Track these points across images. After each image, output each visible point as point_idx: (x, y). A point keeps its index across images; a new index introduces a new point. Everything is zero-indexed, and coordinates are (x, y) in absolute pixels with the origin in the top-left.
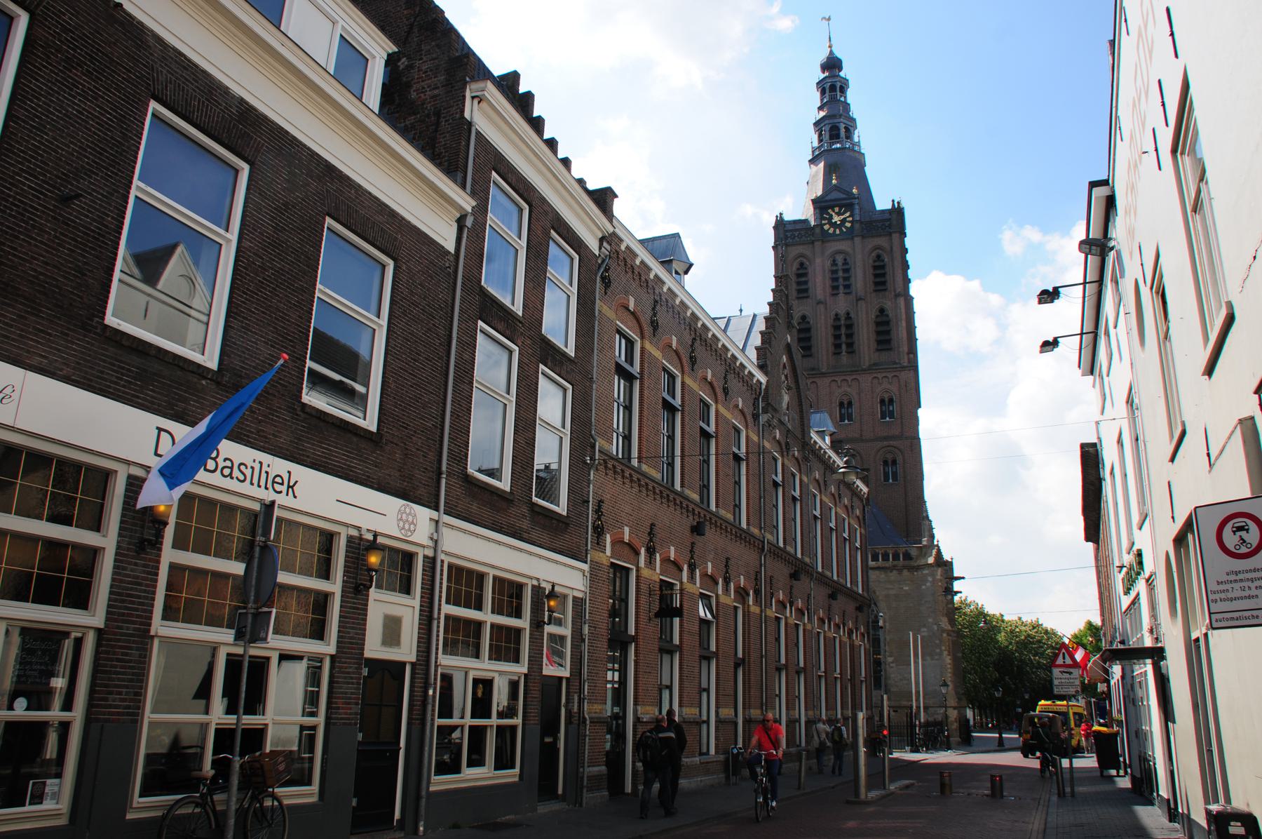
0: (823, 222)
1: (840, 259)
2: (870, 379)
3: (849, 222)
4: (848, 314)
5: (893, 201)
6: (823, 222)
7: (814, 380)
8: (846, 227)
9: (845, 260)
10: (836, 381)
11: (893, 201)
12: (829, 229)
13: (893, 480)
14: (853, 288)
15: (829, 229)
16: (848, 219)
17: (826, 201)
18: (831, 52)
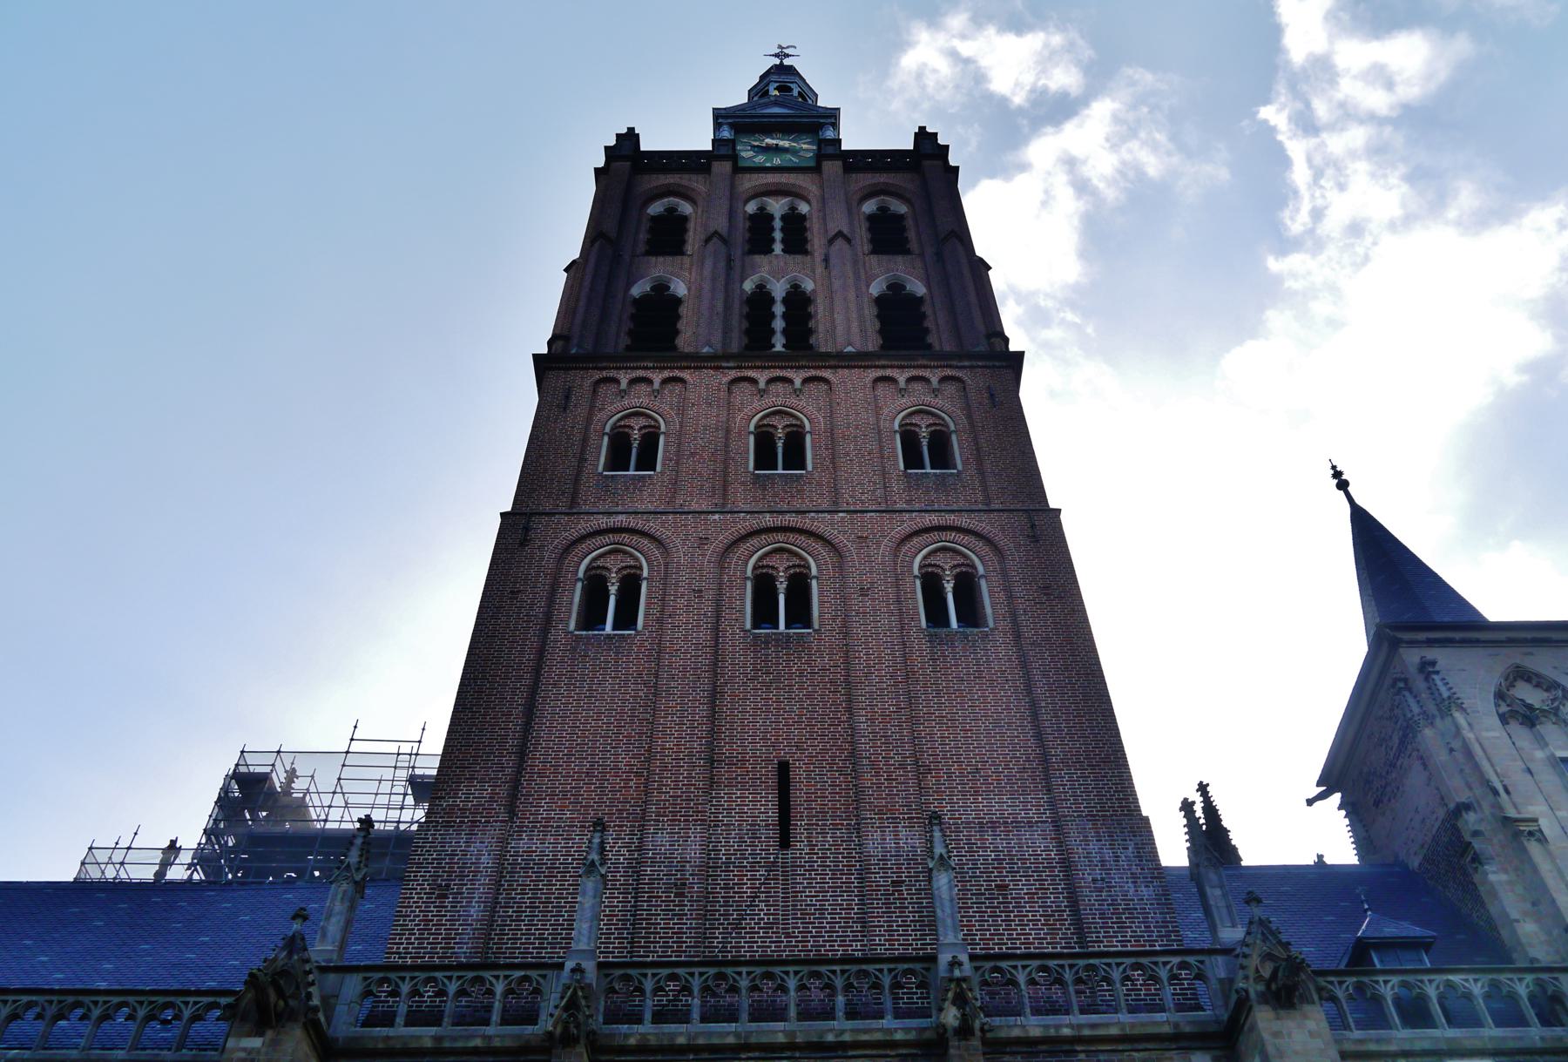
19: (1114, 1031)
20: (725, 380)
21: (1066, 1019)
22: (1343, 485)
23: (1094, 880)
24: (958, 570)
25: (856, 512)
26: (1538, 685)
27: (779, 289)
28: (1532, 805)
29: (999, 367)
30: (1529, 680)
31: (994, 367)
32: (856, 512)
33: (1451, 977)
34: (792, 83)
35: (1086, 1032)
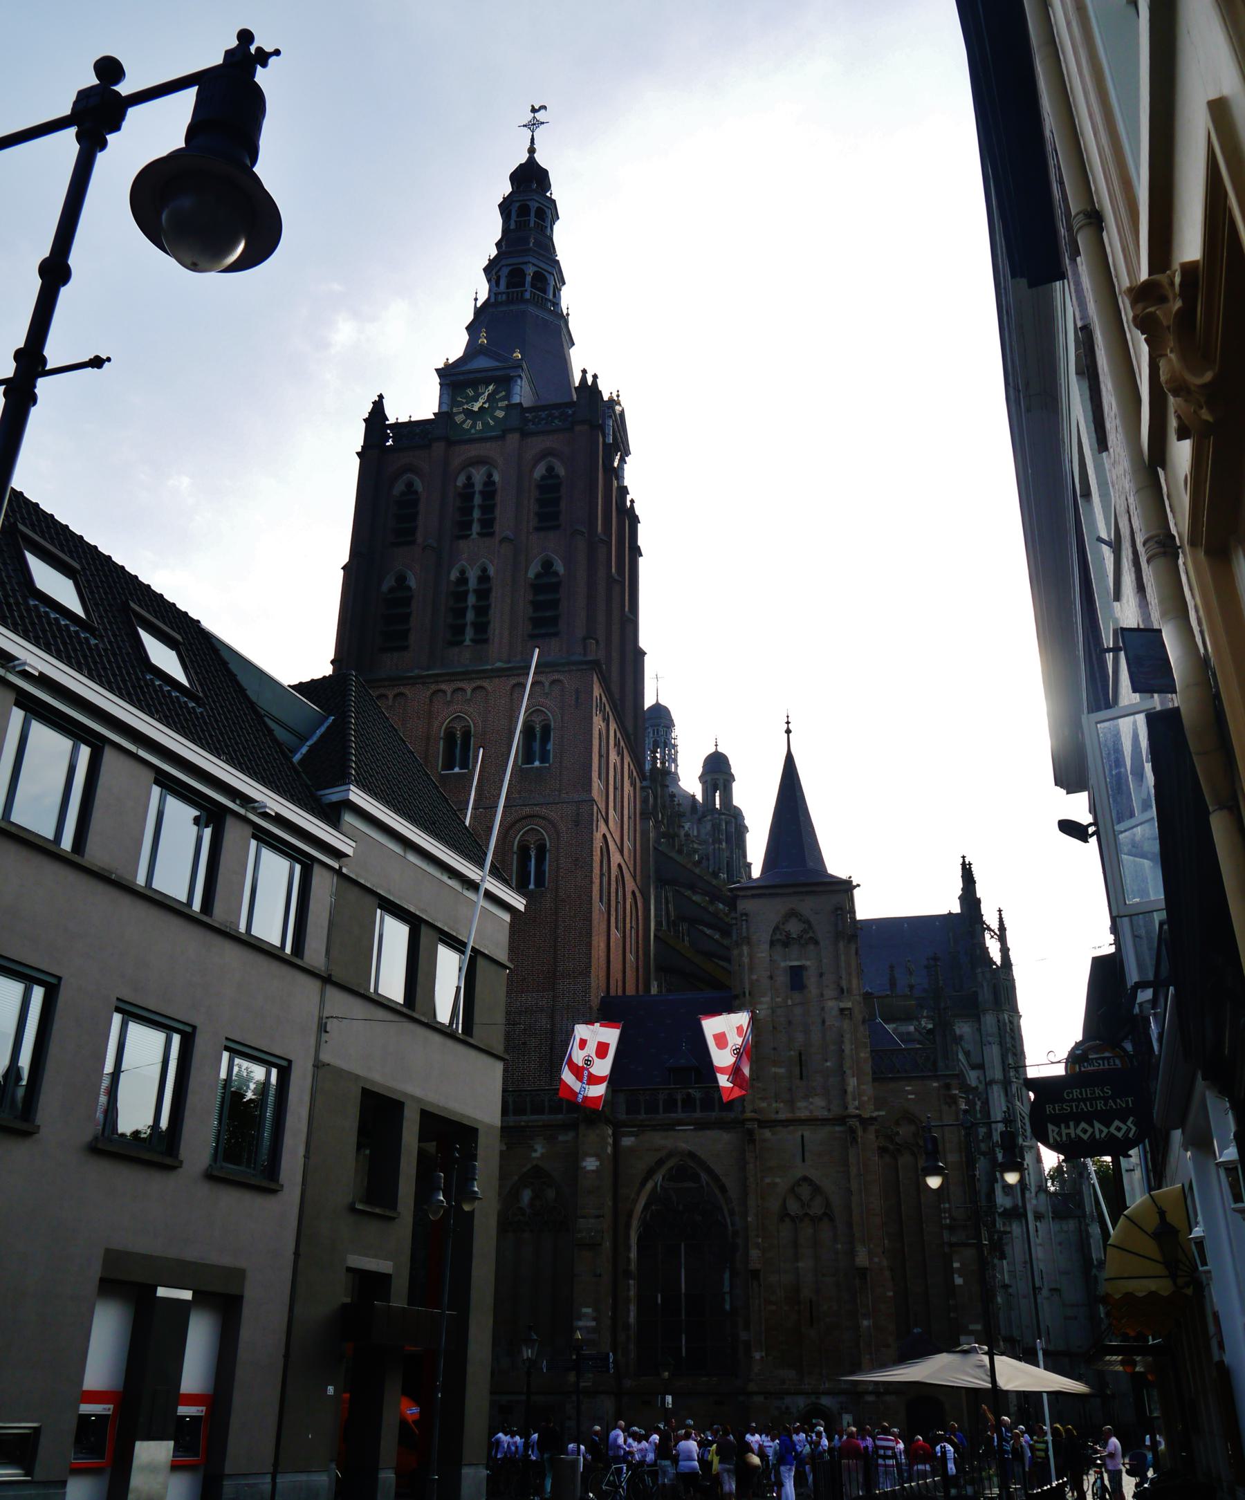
0: (455, 410)
1: (478, 476)
2: (508, 688)
3: (501, 409)
4: (484, 570)
5: (584, 372)
6: (455, 410)
7: (402, 689)
8: (494, 418)
9: (490, 475)
10: (444, 692)
11: (584, 372)
12: (464, 422)
13: (537, 885)
14: (497, 528)
15: (464, 422)
16: (500, 404)
17: (463, 373)
18: (532, 151)
19: (540, 1123)
20: (429, 693)
21: (524, 1118)
22: (788, 732)
23: (561, 1041)
24: (538, 843)
25: (488, 808)
26: (800, 920)
27: (473, 575)
28: (763, 997)
29: (585, 670)
30: (797, 917)
31: (582, 669)
32: (488, 808)
33: (690, 1091)
34: (531, 200)
35: (530, 1124)
